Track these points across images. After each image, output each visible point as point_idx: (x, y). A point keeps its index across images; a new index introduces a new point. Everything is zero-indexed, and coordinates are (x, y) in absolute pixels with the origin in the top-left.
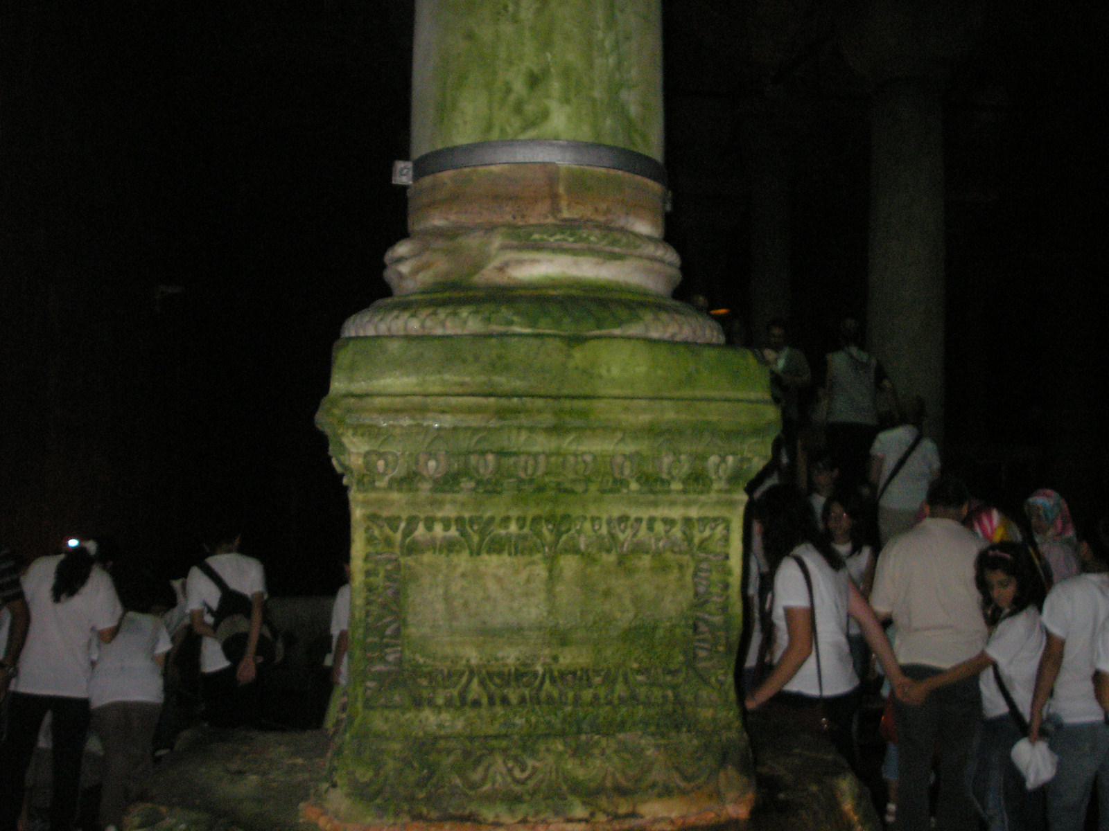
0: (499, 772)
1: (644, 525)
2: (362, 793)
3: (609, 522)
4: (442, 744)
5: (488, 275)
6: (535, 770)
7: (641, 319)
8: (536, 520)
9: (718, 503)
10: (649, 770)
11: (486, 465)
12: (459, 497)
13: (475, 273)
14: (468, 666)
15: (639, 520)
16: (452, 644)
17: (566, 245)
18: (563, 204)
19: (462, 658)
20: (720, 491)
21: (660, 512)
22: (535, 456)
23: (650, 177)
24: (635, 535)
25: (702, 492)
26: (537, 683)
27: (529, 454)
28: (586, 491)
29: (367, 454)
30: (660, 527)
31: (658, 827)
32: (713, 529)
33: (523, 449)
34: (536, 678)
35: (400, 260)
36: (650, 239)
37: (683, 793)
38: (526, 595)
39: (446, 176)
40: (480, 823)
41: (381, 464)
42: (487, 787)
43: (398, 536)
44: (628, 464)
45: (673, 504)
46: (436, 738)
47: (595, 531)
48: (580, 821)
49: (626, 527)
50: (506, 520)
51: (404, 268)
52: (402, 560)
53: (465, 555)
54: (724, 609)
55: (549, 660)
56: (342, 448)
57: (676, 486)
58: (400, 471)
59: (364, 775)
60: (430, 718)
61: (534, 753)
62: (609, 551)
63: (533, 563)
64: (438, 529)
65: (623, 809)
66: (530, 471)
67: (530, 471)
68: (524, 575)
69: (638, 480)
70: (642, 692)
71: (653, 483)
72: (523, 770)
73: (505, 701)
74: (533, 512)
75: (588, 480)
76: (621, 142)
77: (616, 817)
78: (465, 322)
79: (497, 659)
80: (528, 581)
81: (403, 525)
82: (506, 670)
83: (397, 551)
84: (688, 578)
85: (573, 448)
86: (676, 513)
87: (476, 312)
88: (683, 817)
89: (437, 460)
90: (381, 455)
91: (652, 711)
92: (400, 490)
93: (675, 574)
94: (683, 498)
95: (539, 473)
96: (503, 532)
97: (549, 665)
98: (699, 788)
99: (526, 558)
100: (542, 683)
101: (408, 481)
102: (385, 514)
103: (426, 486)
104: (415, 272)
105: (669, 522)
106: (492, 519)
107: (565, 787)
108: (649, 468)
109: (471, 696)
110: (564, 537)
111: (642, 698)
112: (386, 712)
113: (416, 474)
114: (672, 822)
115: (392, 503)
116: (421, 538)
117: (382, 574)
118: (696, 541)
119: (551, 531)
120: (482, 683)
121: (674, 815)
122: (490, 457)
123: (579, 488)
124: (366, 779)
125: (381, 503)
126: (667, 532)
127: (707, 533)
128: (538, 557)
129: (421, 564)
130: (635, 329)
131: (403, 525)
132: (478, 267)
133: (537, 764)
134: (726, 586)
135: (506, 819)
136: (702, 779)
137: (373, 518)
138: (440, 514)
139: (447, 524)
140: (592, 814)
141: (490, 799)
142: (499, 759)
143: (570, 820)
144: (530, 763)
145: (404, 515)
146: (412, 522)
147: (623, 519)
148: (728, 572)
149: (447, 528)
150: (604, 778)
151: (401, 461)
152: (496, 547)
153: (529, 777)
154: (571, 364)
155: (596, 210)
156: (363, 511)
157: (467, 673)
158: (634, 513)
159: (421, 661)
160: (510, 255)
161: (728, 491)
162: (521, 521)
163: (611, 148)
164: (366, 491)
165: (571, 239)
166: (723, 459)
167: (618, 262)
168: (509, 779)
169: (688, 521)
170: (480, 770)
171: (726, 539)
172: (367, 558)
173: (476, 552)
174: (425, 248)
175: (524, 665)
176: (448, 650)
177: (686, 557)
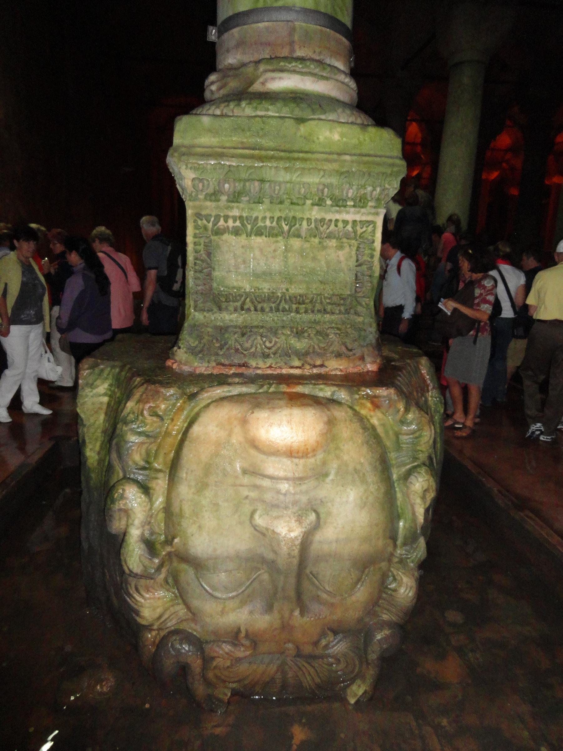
0: (258, 343)
1: (333, 223)
2: (193, 351)
4: (230, 329)
5: (257, 87)
6: (276, 343)
7: (336, 111)
8: (279, 218)
9: (370, 213)
10: (331, 345)
11: (254, 188)
12: (241, 205)
13: (250, 86)
14: (245, 292)
15: (330, 221)
16: (237, 280)
17: (297, 69)
18: (297, 47)
19: (242, 288)
20: (371, 207)
22: (280, 184)
23: (343, 36)
24: (328, 229)
25: (363, 207)
26: (278, 301)
27: (275, 182)
28: (304, 204)
29: (193, 179)
30: (340, 225)
31: (333, 373)
32: (367, 227)
33: (273, 179)
34: (278, 299)
35: (212, 83)
36: (343, 72)
38: (274, 257)
39: (235, 31)
40: (249, 367)
41: (201, 185)
42: (253, 350)
43: (210, 225)
44: (326, 189)
45: (348, 213)
46: (228, 327)
47: (308, 226)
48: (297, 367)
49: (324, 224)
50: (264, 218)
51: (214, 88)
52: (212, 237)
53: (244, 236)
54: (370, 268)
55: (284, 290)
56: (182, 178)
58: (210, 190)
59: (193, 343)
61: (275, 334)
62: (315, 236)
63: (277, 242)
66: (276, 192)
67: (276, 192)
68: (273, 247)
69: (331, 199)
70: (329, 308)
71: (339, 203)
72: (271, 342)
73: (263, 310)
74: (277, 214)
75: (305, 198)
76: (329, 11)
78: (244, 110)
79: (259, 289)
80: (275, 251)
81: (212, 219)
83: (210, 233)
84: (354, 253)
85: (299, 179)
87: (250, 104)
88: (346, 368)
89: (229, 183)
90: (201, 180)
91: (333, 317)
92: (211, 201)
93: (347, 249)
94: (352, 210)
95: (281, 193)
97: (284, 293)
99: (275, 239)
100: (280, 302)
101: (214, 196)
102: (204, 213)
103: (224, 198)
104: (219, 89)
105: (346, 222)
106: (257, 218)
107: (290, 351)
108: (337, 192)
109: (246, 307)
110: (293, 229)
111: (329, 310)
112: (205, 313)
113: (218, 191)
114: (341, 370)
115: (207, 208)
116: (221, 227)
117: (203, 243)
118: (359, 233)
119: (286, 225)
121: (341, 367)
122: (257, 184)
123: (301, 202)
124: (195, 345)
125: (201, 208)
126: (344, 228)
127: (364, 229)
128: (280, 238)
129: (222, 240)
130: (331, 116)
132: (251, 83)
133: (277, 340)
134: (372, 256)
135: (261, 364)
137: (198, 215)
139: (235, 219)
140: (303, 365)
141: (254, 355)
142: (259, 338)
143: (292, 367)
144: (274, 339)
145: (213, 214)
146: (217, 217)
148: (374, 250)
149: (235, 221)
150: (309, 348)
151: (211, 183)
152: (259, 233)
154: (299, 134)
155: (315, 52)
156: (192, 211)
157: (244, 296)
158: (328, 217)
160: (269, 75)
161: (375, 207)
162: (272, 218)
163: (325, 14)
164: (194, 200)
165: (300, 66)
166: (374, 189)
167: (325, 82)
168: (264, 347)
170: (250, 341)
171: (374, 231)
172: (195, 236)
173: (249, 235)
174: (224, 77)
175: (273, 293)
176: (235, 284)
177: (353, 241)
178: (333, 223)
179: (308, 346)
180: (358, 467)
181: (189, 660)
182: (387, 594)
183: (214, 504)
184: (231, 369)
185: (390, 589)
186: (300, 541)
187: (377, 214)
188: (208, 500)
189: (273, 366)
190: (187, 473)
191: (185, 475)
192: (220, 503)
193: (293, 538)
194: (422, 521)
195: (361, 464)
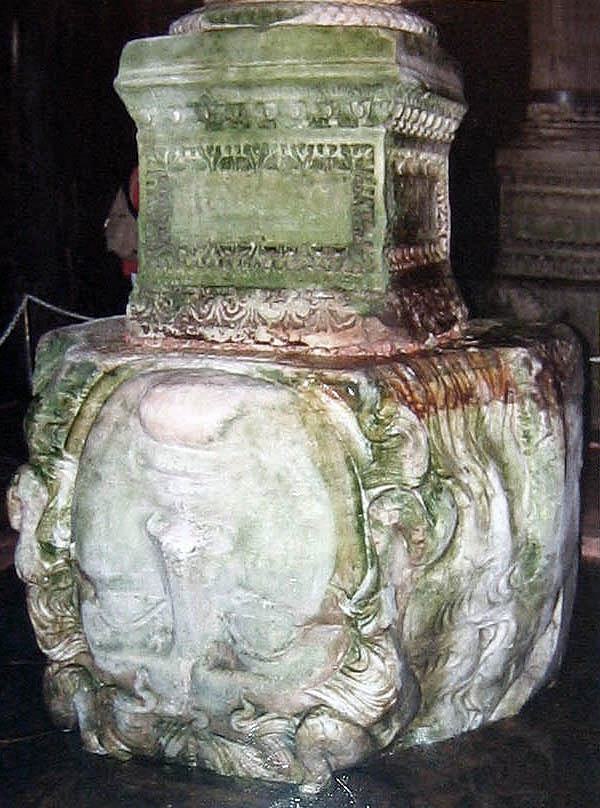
3: (293, 147)
15: (312, 146)
21: (328, 141)
30: (327, 151)
31: (317, 352)
37: (335, 330)
45: (334, 135)
57: (333, 122)
60: (181, 271)
64: (188, 153)
65: (294, 338)
77: (291, 344)
82: (232, 245)
86: (338, 141)
98: (346, 327)
100: (254, 253)
105: (334, 148)
109: (208, 261)
114: (327, 350)
120: (218, 252)
121: (328, 347)
136: (349, 323)
138: (188, 146)
140: (272, 340)
141: (212, 324)
143: (258, 343)
149: (193, 153)
153: (237, 313)
169: (344, 146)
179: (283, 315)
180: (283, 473)
184: (185, 343)
187: (374, 135)
189: (233, 339)
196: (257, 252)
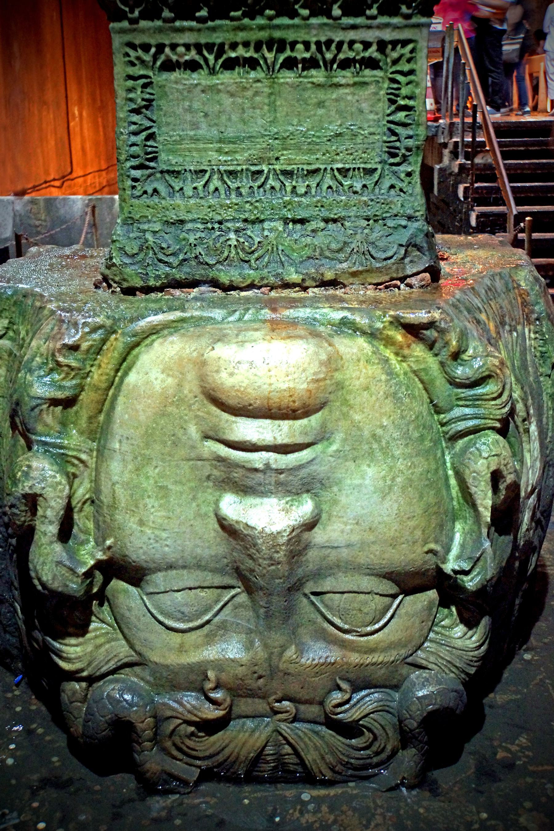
1: (345, 46)
45: (369, 27)
93: (372, 89)
96: (233, 55)
100: (267, 178)
105: (367, 45)
131: (153, 50)
138: (181, 41)
147: (329, 43)
159: (173, 162)
173: (212, 72)
178: (345, 46)
180: (379, 432)
181: (133, 718)
182: (437, 633)
183: (161, 487)
185: (443, 627)
186: (286, 538)
188: (152, 481)
190: (120, 442)
191: (117, 446)
192: (170, 487)
193: (275, 533)
194: (489, 519)
195: (382, 427)
196: (271, 176)
